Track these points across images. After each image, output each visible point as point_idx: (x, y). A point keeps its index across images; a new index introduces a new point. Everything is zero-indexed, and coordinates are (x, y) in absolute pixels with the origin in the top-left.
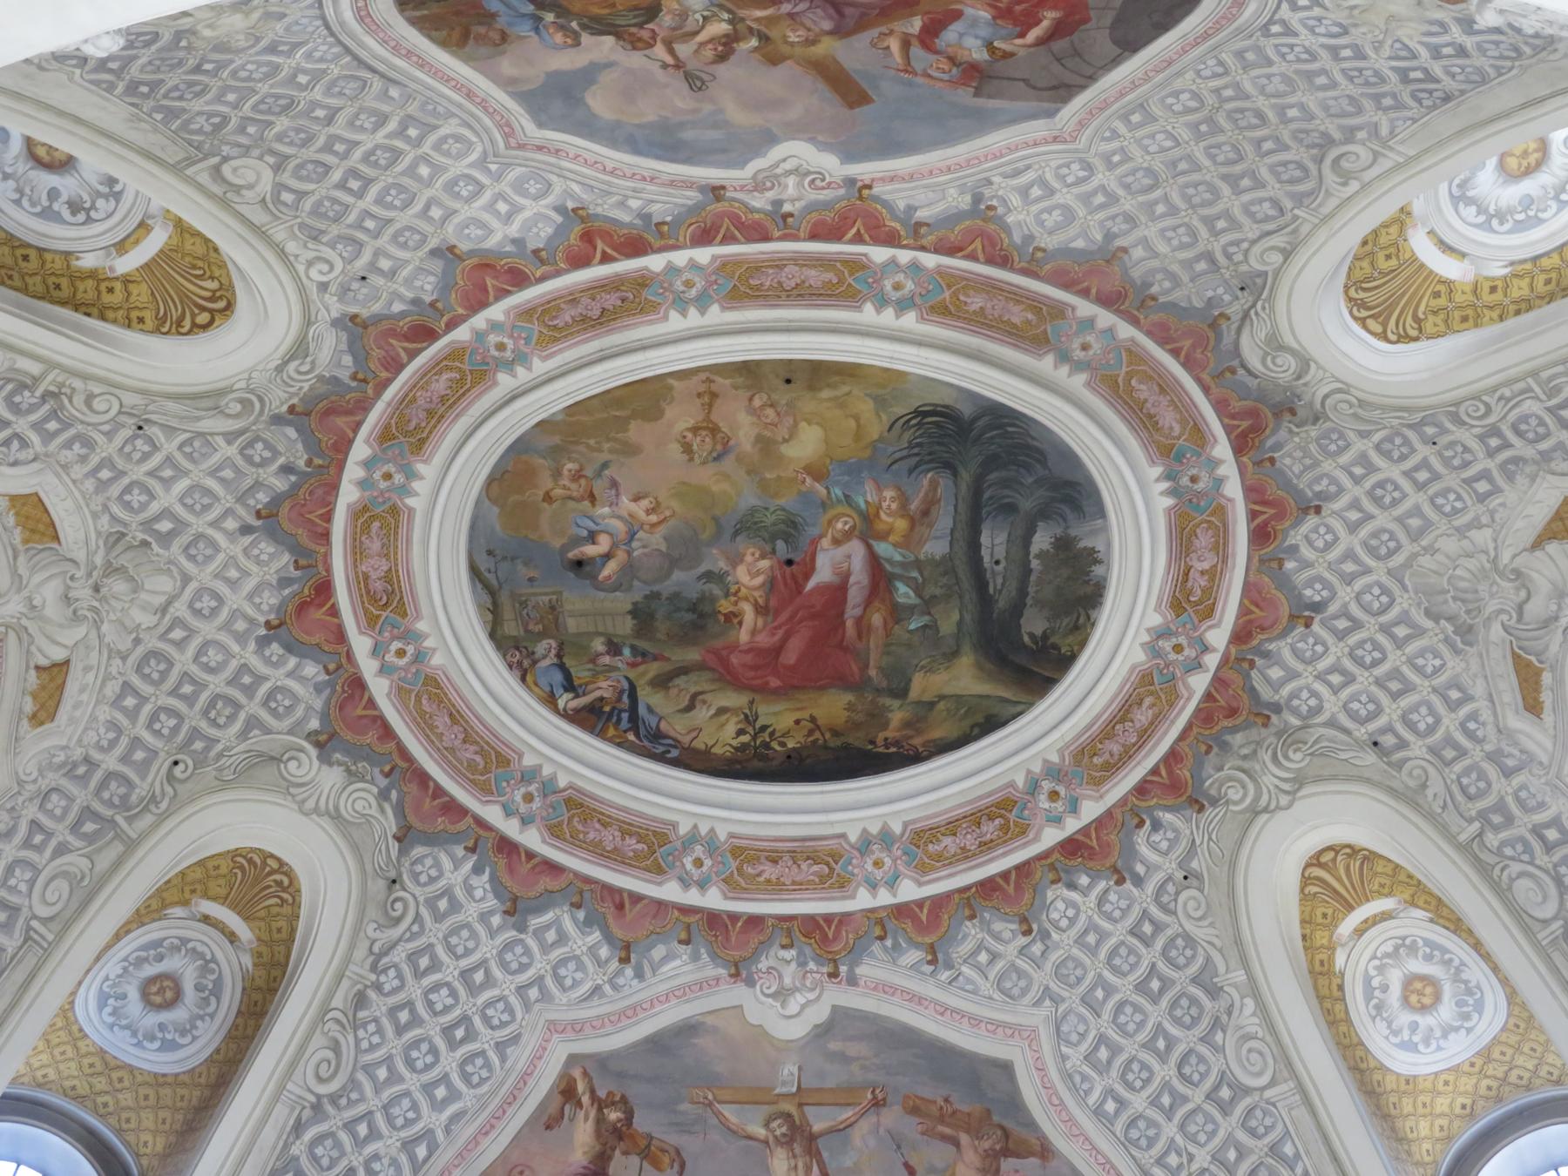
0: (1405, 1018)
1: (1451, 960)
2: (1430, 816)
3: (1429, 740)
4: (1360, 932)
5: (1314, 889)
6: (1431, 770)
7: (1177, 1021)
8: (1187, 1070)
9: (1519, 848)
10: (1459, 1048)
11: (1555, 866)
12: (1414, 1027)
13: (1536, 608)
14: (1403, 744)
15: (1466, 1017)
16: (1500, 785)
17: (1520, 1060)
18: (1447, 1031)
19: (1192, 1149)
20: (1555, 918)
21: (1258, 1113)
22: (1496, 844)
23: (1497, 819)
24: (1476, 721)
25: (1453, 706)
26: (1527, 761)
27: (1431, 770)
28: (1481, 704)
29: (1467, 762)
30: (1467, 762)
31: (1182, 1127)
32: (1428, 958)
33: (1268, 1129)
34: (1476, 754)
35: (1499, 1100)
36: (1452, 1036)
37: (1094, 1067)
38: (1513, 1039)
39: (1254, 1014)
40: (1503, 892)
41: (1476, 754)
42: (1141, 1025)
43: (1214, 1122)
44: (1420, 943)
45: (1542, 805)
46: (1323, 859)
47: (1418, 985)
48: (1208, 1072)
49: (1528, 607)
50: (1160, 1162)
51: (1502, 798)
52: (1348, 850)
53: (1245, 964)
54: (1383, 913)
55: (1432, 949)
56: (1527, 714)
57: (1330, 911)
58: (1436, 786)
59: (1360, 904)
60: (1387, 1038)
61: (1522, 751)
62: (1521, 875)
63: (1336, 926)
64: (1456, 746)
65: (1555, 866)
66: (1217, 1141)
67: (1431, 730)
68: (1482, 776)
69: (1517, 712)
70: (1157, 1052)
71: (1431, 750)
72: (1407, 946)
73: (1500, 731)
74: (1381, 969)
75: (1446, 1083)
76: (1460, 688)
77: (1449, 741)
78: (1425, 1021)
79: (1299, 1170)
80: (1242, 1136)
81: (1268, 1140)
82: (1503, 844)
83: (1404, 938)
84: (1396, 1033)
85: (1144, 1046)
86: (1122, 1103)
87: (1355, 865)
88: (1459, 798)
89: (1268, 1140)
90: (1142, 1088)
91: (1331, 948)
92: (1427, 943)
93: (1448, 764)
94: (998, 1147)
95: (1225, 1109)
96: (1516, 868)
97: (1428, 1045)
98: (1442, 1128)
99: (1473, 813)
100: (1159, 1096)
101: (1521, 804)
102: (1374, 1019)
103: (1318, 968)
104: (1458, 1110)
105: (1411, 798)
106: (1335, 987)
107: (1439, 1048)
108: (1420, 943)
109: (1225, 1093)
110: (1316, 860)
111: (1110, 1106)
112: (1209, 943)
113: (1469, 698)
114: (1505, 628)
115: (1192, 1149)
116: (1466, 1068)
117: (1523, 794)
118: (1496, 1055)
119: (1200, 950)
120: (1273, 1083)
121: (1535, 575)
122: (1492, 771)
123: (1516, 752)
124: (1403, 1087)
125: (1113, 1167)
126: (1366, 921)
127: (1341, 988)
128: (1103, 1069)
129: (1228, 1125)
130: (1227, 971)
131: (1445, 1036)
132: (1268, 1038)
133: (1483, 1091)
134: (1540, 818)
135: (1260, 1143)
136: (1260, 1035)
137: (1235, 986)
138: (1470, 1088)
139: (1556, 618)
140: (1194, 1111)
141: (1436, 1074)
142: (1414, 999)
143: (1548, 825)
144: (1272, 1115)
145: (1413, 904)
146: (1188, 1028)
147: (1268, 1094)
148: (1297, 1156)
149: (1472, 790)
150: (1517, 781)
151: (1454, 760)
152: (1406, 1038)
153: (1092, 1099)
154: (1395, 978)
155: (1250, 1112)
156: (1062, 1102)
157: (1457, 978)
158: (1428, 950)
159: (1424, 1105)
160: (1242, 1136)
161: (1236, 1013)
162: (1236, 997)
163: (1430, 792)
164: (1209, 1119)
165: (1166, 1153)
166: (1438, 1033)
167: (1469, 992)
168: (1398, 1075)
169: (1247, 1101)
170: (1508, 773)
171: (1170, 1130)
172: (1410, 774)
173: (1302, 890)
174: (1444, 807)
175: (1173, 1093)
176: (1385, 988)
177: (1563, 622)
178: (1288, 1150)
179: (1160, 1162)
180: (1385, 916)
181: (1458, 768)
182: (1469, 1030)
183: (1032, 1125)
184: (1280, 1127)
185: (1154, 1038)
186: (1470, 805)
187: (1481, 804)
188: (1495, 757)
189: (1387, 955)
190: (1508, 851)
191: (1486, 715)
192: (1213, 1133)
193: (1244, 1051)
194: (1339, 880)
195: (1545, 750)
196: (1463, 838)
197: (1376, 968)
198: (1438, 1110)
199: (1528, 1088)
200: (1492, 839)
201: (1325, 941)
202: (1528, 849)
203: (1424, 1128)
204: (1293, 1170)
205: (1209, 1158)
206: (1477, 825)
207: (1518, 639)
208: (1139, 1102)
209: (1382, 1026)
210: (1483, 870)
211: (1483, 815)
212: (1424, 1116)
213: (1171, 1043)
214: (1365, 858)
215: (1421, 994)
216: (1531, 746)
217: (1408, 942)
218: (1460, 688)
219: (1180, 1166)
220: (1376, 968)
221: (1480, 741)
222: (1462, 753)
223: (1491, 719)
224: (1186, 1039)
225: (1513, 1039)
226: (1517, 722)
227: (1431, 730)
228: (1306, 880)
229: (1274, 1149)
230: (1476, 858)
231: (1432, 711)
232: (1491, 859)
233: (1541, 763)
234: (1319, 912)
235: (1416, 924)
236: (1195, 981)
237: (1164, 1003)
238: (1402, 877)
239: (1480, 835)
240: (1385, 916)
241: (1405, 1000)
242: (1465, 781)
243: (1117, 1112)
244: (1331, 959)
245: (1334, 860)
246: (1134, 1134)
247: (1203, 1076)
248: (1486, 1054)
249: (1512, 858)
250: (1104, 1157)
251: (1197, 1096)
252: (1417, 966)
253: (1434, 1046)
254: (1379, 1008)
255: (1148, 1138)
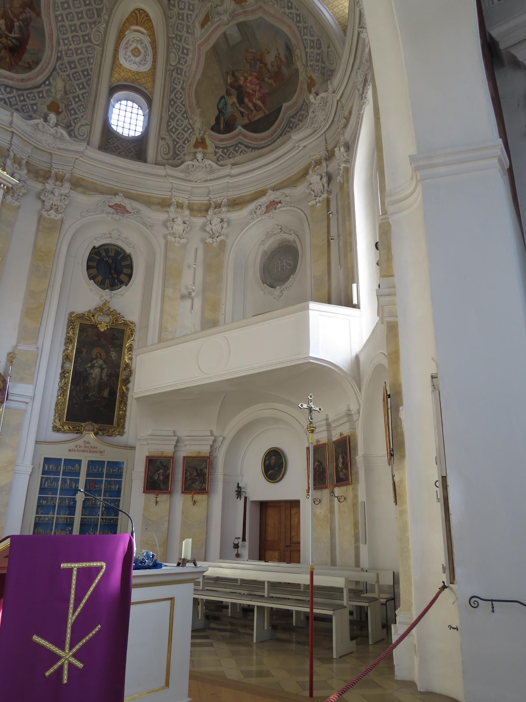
0: (129, 54)
1: (147, 52)
2: (167, 25)
3: (179, 11)
4: (135, 31)
5: (133, 14)
6: (175, 17)
7: (87, 14)
8: (82, 26)
9: (178, 47)
10: (134, 68)
11: (181, 57)
12: (129, 57)
13: (220, 9)
14: (174, 6)
15: (140, 64)
16: (184, 33)
17: (143, 80)
18: (135, 63)
19: (72, 43)
20: (173, 66)
21: (90, 48)
22: (174, 42)
23: (178, 38)
24: (191, 17)
25: (189, 9)
26: (193, 34)
27: (175, 17)
28: (194, 15)
29: (182, 22)
30: (182, 22)
31: (73, 37)
32: (143, 48)
33: (90, 53)
34: (185, 23)
35: (133, 82)
36: (135, 65)
37: (62, 7)
38: (145, 75)
39: (103, 28)
40: (168, 52)
41: (185, 23)
42: (78, 7)
43: (80, 42)
44: (144, 44)
45: (188, 44)
46: (141, 11)
47: (137, 50)
48: (86, 30)
49: (218, 7)
50: (63, 39)
51: (183, 36)
52: (147, 15)
53: (109, 16)
54: (142, 32)
55: (145, 47)
56: (200, 26)
57: (133, 22)
58: (173, 21)
59: (140, 26)
60: (123, 54)
61: (194, 31)
62: (174, 53)
63: (132, 26)
64: (183, 17)
65: (181, 57)
66: (78, 46)
67: (181, 9)
68: (183, 28)
69: (199, 24)
70: (78, 16)
71: (178, 13)
72: (141, 42)
73: (193, 23)
74: (133, 41)
75: (126, 71)
76: (193, 7)
77: (183, 15)
78: (132, 57)
79: (91, 66)
80: (84, 50)
81: (89, 55)
82: (176, 44)
83: (142, 40)
84: (125, 55)
85: (76, 12)
86: (63, 20)
87: (145, 18)
88: (175, 27)
89: (89, 55)
90: (69, 21)
91: (127, 29)
92: (145, 45)
93: (179, 19)
94: (28, 4)
95: (85, 41)
96: (174, 50)
97: (129, 62)
98: (119, 78)
99: (175, 33)
100: (72, 26)
101: (185, 40)
102: (124, 49)
103: (122, 30)
104: (124, 77)
105: (167, 18)
106: (122, 36)
107: (130, 64)
108: (144, 44)
109: (87, 38)
110: (139, 10)
111: (60, 18)
112: (105, 5)
113: (193, 11)
114: (211, 6)
115: (72, 43)
116: (132, 72)
117: (187, 39)
118: (139, 75)
119: (102, 5)
120: (97, 45)
121: (225, 3)
122: (185, 29)
123: (192, 30)
124: (119, 65)
125: (52, 32)
126: (138, 30)
127: (123, 38)
128: (64, 9)
129: (82, 45)
130: (105, 14)
131: (133, 63)
132: (103, 35)
133: (132, 78)
134: (186, 46)
135: (87, 55)
136: (102, 33)
137: (104, 19)
138: (130, 76)
139: (221, 15)
140: (77, 36)
141: (126, 68)
142: (134, 52)
143: (186, 49)
144: (93, 51)
145: (149, 36)
146: (88, 18)
147: (95, 46)
148: (92, 63)
149: (179, 28)
150: (188, 35)
151: (181, 19)
152: (126, 57)
153: (57, 13)
154: (134, 45)
155: (89, 47)
156: (49, 8)
157: (145, 56)
158: (144, 46)
159: (120, 72)
160: (84, 50)
161: (100, 24)
162: (103, 21)
163: (171, 20)
164: (79, 40)
165: (66, 39)
166: (133, 62)
167: (145, 60)
168: (120, 62)
169: (90, 44)
170: (188, 32)
171: (70, 35)
172: (171, 13)
173: (131, 13)
174: (172, 26)
175: (76, 28)
176: (130, 45)
177: (222, 17)
178: (91, 61)
179: (63, 39)
180: (142, 33)
181: (180, 21)
182: (139, 66)
183: (39, 6)
184: (93, 55)
185: (79, 13)
186: (176, 31)
187: (178, 33)
188: (188, 27)
189: (136, 40)
190: (175, 46)
191: (193, 17)
192: (78, 44)
193: (96, 34)
194: (140, 19)
195: (197, 35)
196: (170, 35)
197: (132, 40)
198: (121, 75)
199: (140, 85)
200: (174, 41)
201: (127, 26)
202: (179, 49)
203: (116, 75)
204: (90, 65)
205: (74, 48)
206: (174, 36)
207: (211, 10)
208: (67, 23)
209: (124, 51)
210: (168, 45)
211: (177, 35)
212: (118, 74)
213: (82, 17)
214: (148, 19)
215: (136, 52)
216: (196, 32)
217: (142, 41)
218: (193, 7)
219: (67, 44)
220: (132, 40)
221: (188, 21)
222: (183, 20)
223: (193, 19)
224: (86, 20)
225: (145, 75)
226: (197, 25)
227: (181, 9)
228: (134, 12)
229: (89, 58)
230: (169, 42)
231: (185, 6)
232: (171, 44)
233: (195, 37)
234: (131, 20)
235: (147, 40)
236: (97, 9)
237: (87, 8)
238: (152, 30)
239: (173, 38)
240: (142, 33)
241: (132, 51)
242: (179, 25)
243: (61, 21)
244: (125, 31)
245: (142, 13)
246: (61, 29)
247: (84, 31)
248: (138, 73)
249: (175, 48)
250: (52, 28)
251: (80, 34)
252: (140, 47)
253: (130, 63)
254: (127, 47)
255: (64, 33)
